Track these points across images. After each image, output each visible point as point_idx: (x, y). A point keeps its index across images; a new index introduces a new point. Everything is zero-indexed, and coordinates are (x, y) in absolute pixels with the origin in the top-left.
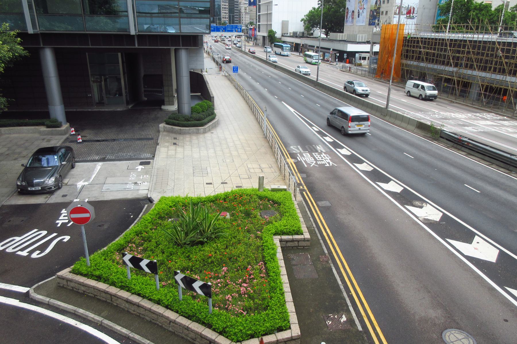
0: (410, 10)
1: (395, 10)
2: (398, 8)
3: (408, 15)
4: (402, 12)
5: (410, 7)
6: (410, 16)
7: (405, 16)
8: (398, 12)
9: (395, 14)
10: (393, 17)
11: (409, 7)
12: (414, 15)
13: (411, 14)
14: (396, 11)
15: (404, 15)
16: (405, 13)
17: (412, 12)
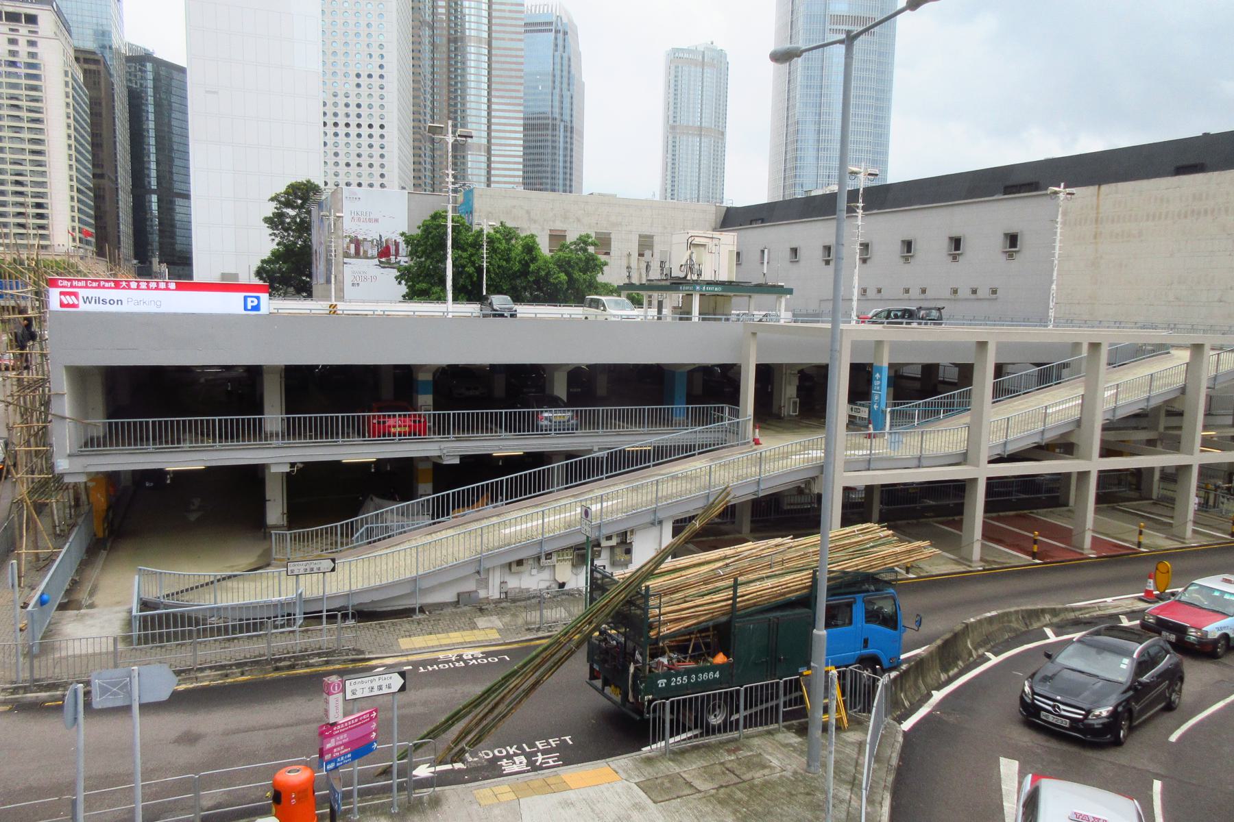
0: (388, 248)
1: (345, 246)
2: (351, 241)
3: (383, 260)
4: (365, 252)
5: (387, 241)
6: (388, 262)
7: (376, 261)
8: (352, 251)
9: (347, 255)
10: (342, 264)
11: (383, 240)
12: (399, 258)
13: (393, 258)
14: (348, 248)
15: (372, 258)
16: (375, 253)
17: (393, 251)
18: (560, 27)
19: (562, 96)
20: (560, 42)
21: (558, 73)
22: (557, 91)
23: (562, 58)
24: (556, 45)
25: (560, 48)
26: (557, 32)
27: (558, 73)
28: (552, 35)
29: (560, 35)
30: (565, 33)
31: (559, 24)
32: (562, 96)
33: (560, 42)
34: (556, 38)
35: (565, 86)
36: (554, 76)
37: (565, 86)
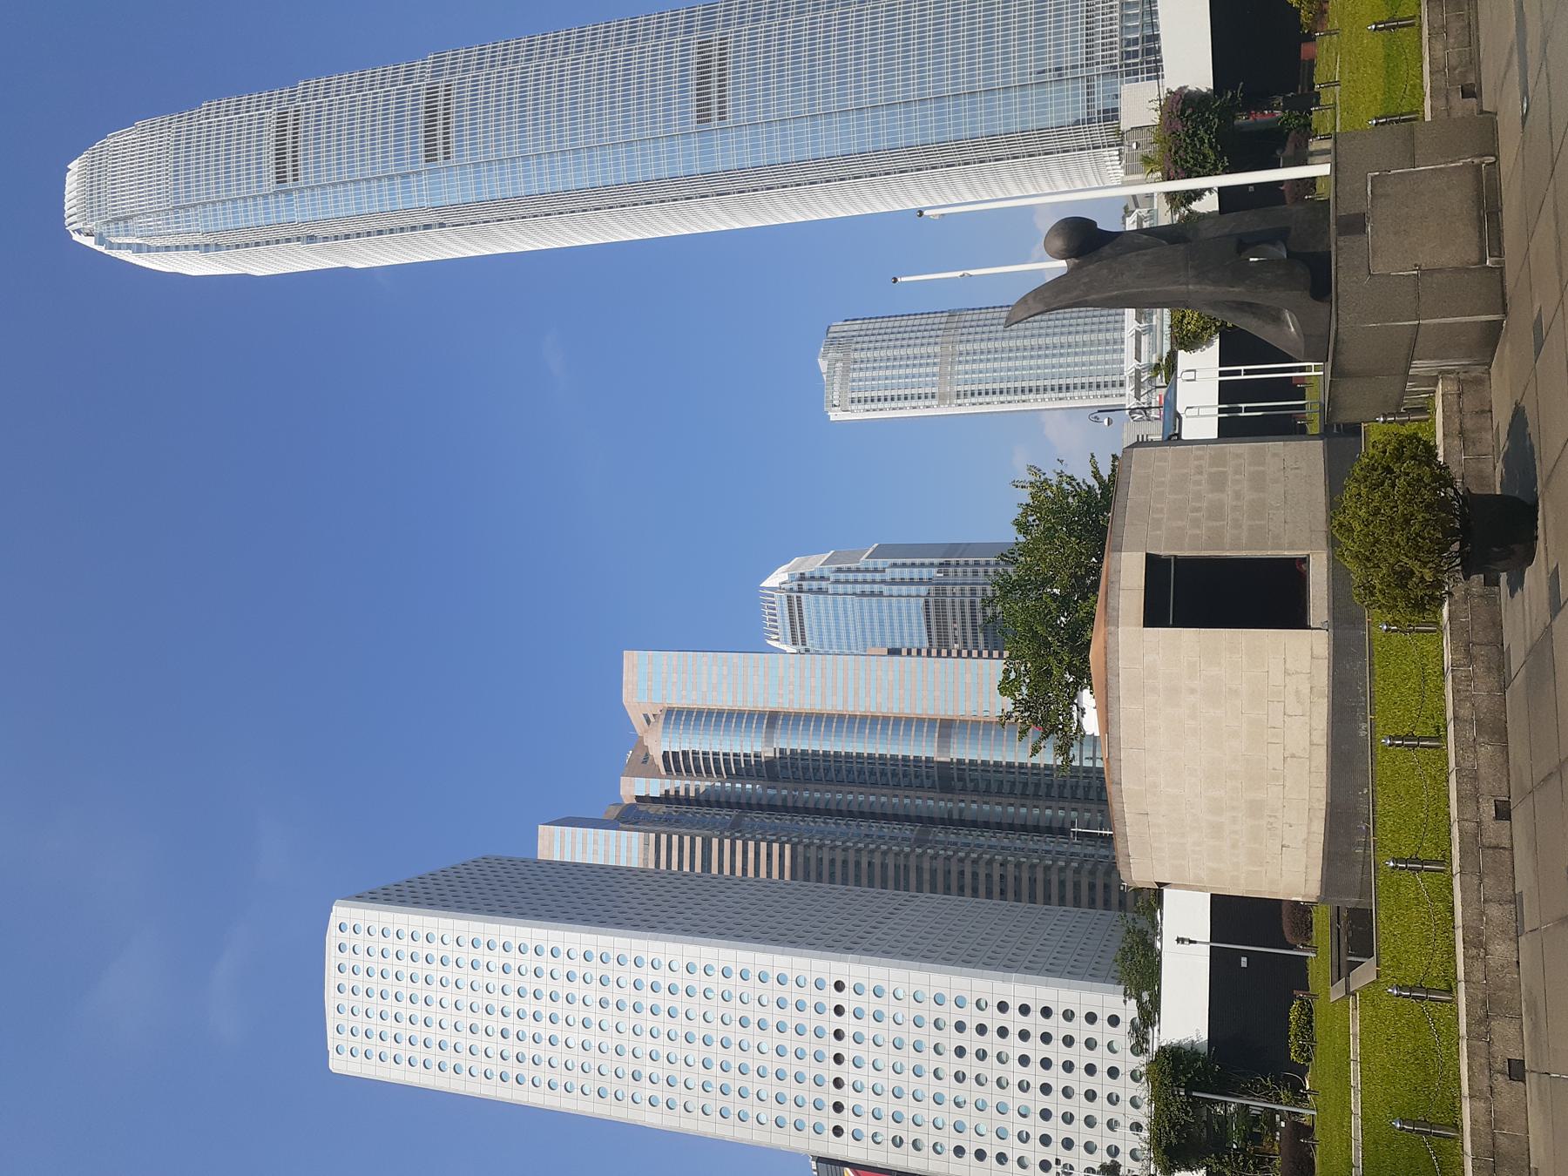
18: (795, 585)
19: (893, 582)
20: (815, 585)
21: (859, 588)
22: (885, 589)
23: (837, 582)
24: (820, 591)
25: (824, 584)
26: (801, 590)
27: (859, 588)
28: (803, 596)
29: (805, 585)
30: (802, 577)
31: (787, 586)
32: (893, 582)
33: (815, 585)
34: (810, 591)
35: (878, 577)
36: (863, 594)
37: (878, 577)
